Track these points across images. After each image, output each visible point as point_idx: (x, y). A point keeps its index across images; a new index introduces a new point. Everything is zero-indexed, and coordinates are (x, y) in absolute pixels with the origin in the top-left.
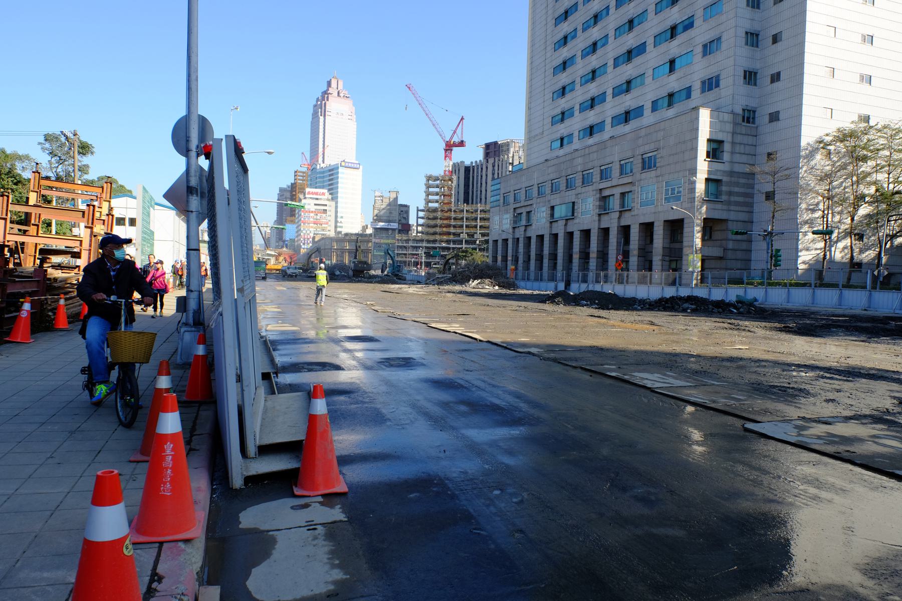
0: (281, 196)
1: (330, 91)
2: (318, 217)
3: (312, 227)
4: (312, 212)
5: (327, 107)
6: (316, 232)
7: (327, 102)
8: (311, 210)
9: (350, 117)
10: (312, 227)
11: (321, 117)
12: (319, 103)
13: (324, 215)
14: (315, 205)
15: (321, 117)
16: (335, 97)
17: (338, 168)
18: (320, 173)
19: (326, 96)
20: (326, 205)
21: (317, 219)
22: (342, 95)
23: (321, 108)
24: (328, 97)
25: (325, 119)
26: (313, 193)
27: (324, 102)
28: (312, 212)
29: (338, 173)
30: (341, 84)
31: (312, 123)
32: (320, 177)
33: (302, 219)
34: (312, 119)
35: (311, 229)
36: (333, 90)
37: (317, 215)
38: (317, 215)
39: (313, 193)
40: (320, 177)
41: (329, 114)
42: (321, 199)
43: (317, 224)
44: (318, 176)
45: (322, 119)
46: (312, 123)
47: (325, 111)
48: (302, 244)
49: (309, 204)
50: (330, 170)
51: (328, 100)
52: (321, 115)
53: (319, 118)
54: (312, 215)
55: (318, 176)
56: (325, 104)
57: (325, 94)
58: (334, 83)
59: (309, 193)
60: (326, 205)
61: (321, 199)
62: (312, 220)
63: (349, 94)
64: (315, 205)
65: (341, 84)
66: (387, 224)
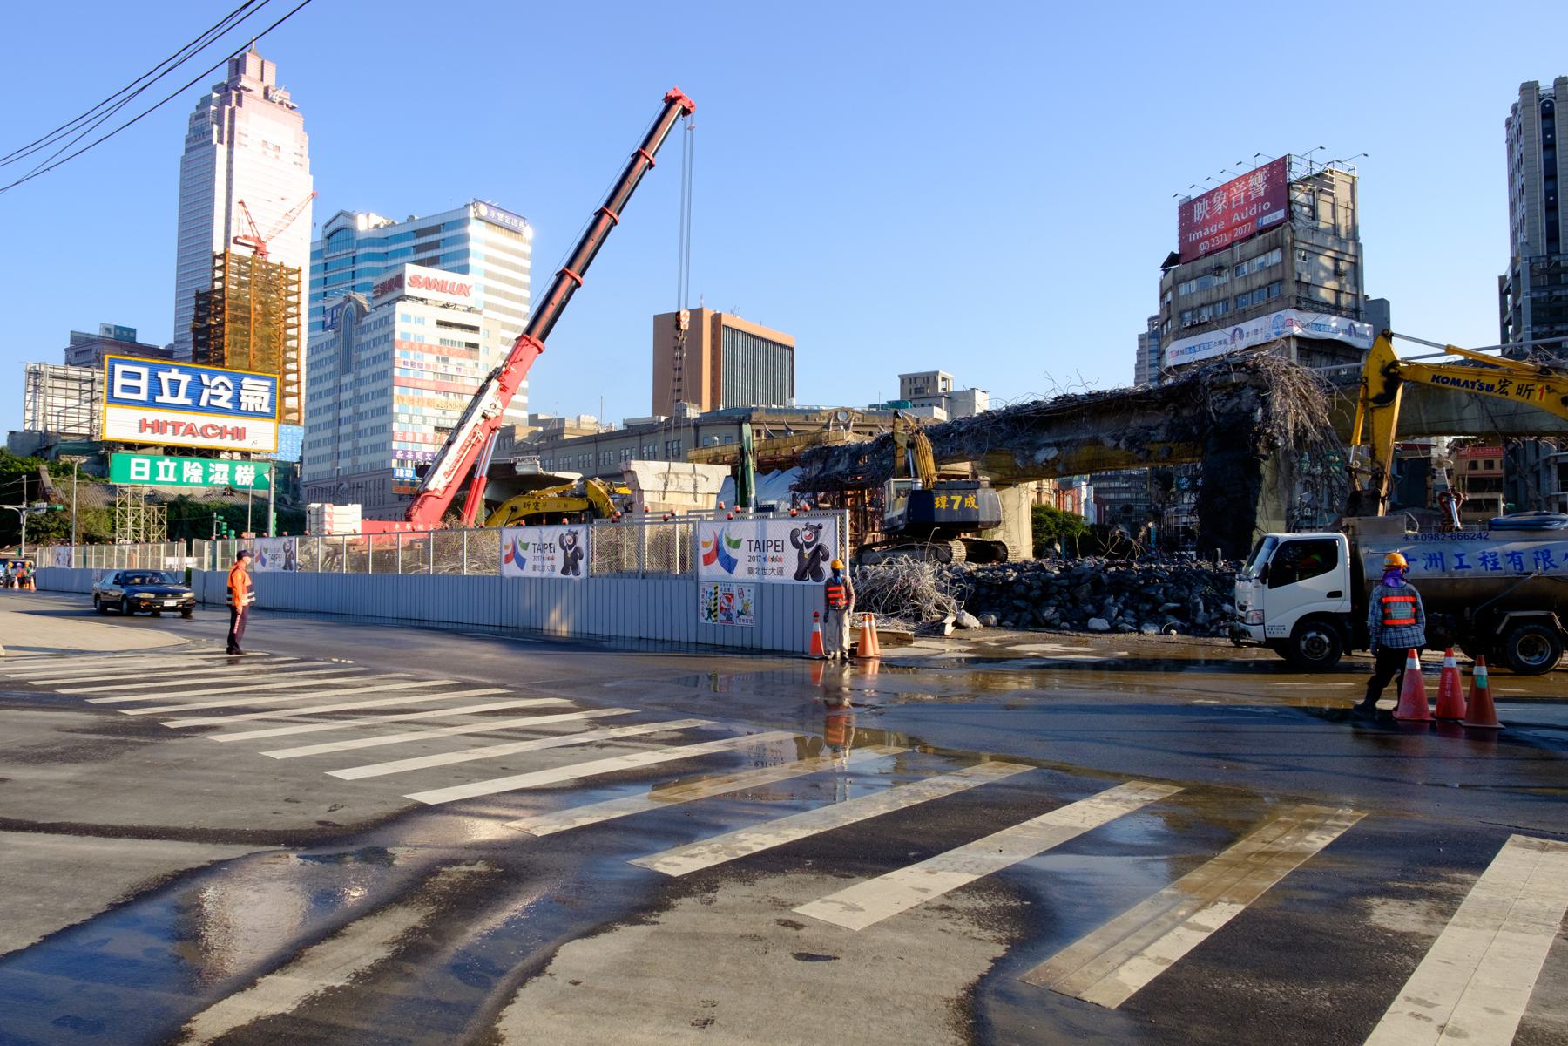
0: (77, 354)
1: (244, 82)
2: (451, 370)
3: (430, 403)
4: (430, 350)
5: (238, 123)
6: (442, 424)
7: (238, 110)
8: (428, 341)
9: (297, 159)
10: (430, 403)
11: (219, 146)
12: (213, 108)
13: (469, 363)
14: (441, 323)
15: (219, 146)
16: (253, 97)
17: (464, 222)
18: (371, 241)
19: (234, 93)
20: (474, 329)
21: (447, 376)
22: (276, 96)
23: (221, 125)
24: (239, 98)
25: (230, 153)
26: (429, 284)
27: (227, 108)
28: (430, 350)
29: (465, 238)
30: (270, 70)
31: (184, 162)
32: (370, 257)
33: (397, 372)
34: (188, 151)
35: (427, 411)
36: (249, 79)
37: (445, 360)
38: (445, 360)
39: (429, 284)
40: (370, 257)
41: (244, 140)
42: (454, 307)
43: (446, 393)
44: (361, 251)
45: (222, 151)
46: (185, 162)
47: (231, 133)
48: (394, 463)
49: (420, 320)
50: (419, 233)
51: (239, 103)
52: (221, 141)
53: (214, 148)
54: (430, 359)
55: (361, 251)
56: (232, 112)
57: (230, 90)
58: (252, 64)
59: (416, 281)
60: (474, 329)
61: (454, 307)
62: (429, 376)
63: (291, 101)
64: (441, 323)
65: (270, 70)
66: (1346, 323)
